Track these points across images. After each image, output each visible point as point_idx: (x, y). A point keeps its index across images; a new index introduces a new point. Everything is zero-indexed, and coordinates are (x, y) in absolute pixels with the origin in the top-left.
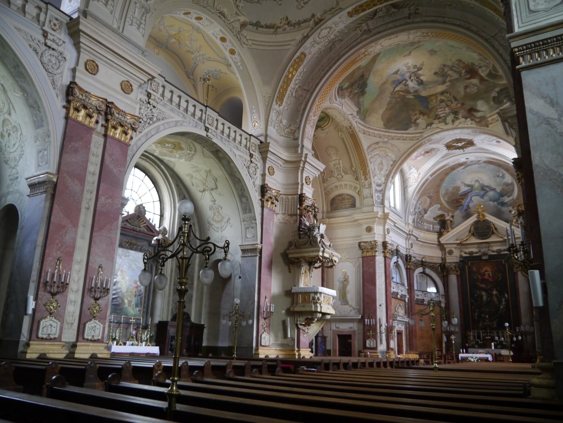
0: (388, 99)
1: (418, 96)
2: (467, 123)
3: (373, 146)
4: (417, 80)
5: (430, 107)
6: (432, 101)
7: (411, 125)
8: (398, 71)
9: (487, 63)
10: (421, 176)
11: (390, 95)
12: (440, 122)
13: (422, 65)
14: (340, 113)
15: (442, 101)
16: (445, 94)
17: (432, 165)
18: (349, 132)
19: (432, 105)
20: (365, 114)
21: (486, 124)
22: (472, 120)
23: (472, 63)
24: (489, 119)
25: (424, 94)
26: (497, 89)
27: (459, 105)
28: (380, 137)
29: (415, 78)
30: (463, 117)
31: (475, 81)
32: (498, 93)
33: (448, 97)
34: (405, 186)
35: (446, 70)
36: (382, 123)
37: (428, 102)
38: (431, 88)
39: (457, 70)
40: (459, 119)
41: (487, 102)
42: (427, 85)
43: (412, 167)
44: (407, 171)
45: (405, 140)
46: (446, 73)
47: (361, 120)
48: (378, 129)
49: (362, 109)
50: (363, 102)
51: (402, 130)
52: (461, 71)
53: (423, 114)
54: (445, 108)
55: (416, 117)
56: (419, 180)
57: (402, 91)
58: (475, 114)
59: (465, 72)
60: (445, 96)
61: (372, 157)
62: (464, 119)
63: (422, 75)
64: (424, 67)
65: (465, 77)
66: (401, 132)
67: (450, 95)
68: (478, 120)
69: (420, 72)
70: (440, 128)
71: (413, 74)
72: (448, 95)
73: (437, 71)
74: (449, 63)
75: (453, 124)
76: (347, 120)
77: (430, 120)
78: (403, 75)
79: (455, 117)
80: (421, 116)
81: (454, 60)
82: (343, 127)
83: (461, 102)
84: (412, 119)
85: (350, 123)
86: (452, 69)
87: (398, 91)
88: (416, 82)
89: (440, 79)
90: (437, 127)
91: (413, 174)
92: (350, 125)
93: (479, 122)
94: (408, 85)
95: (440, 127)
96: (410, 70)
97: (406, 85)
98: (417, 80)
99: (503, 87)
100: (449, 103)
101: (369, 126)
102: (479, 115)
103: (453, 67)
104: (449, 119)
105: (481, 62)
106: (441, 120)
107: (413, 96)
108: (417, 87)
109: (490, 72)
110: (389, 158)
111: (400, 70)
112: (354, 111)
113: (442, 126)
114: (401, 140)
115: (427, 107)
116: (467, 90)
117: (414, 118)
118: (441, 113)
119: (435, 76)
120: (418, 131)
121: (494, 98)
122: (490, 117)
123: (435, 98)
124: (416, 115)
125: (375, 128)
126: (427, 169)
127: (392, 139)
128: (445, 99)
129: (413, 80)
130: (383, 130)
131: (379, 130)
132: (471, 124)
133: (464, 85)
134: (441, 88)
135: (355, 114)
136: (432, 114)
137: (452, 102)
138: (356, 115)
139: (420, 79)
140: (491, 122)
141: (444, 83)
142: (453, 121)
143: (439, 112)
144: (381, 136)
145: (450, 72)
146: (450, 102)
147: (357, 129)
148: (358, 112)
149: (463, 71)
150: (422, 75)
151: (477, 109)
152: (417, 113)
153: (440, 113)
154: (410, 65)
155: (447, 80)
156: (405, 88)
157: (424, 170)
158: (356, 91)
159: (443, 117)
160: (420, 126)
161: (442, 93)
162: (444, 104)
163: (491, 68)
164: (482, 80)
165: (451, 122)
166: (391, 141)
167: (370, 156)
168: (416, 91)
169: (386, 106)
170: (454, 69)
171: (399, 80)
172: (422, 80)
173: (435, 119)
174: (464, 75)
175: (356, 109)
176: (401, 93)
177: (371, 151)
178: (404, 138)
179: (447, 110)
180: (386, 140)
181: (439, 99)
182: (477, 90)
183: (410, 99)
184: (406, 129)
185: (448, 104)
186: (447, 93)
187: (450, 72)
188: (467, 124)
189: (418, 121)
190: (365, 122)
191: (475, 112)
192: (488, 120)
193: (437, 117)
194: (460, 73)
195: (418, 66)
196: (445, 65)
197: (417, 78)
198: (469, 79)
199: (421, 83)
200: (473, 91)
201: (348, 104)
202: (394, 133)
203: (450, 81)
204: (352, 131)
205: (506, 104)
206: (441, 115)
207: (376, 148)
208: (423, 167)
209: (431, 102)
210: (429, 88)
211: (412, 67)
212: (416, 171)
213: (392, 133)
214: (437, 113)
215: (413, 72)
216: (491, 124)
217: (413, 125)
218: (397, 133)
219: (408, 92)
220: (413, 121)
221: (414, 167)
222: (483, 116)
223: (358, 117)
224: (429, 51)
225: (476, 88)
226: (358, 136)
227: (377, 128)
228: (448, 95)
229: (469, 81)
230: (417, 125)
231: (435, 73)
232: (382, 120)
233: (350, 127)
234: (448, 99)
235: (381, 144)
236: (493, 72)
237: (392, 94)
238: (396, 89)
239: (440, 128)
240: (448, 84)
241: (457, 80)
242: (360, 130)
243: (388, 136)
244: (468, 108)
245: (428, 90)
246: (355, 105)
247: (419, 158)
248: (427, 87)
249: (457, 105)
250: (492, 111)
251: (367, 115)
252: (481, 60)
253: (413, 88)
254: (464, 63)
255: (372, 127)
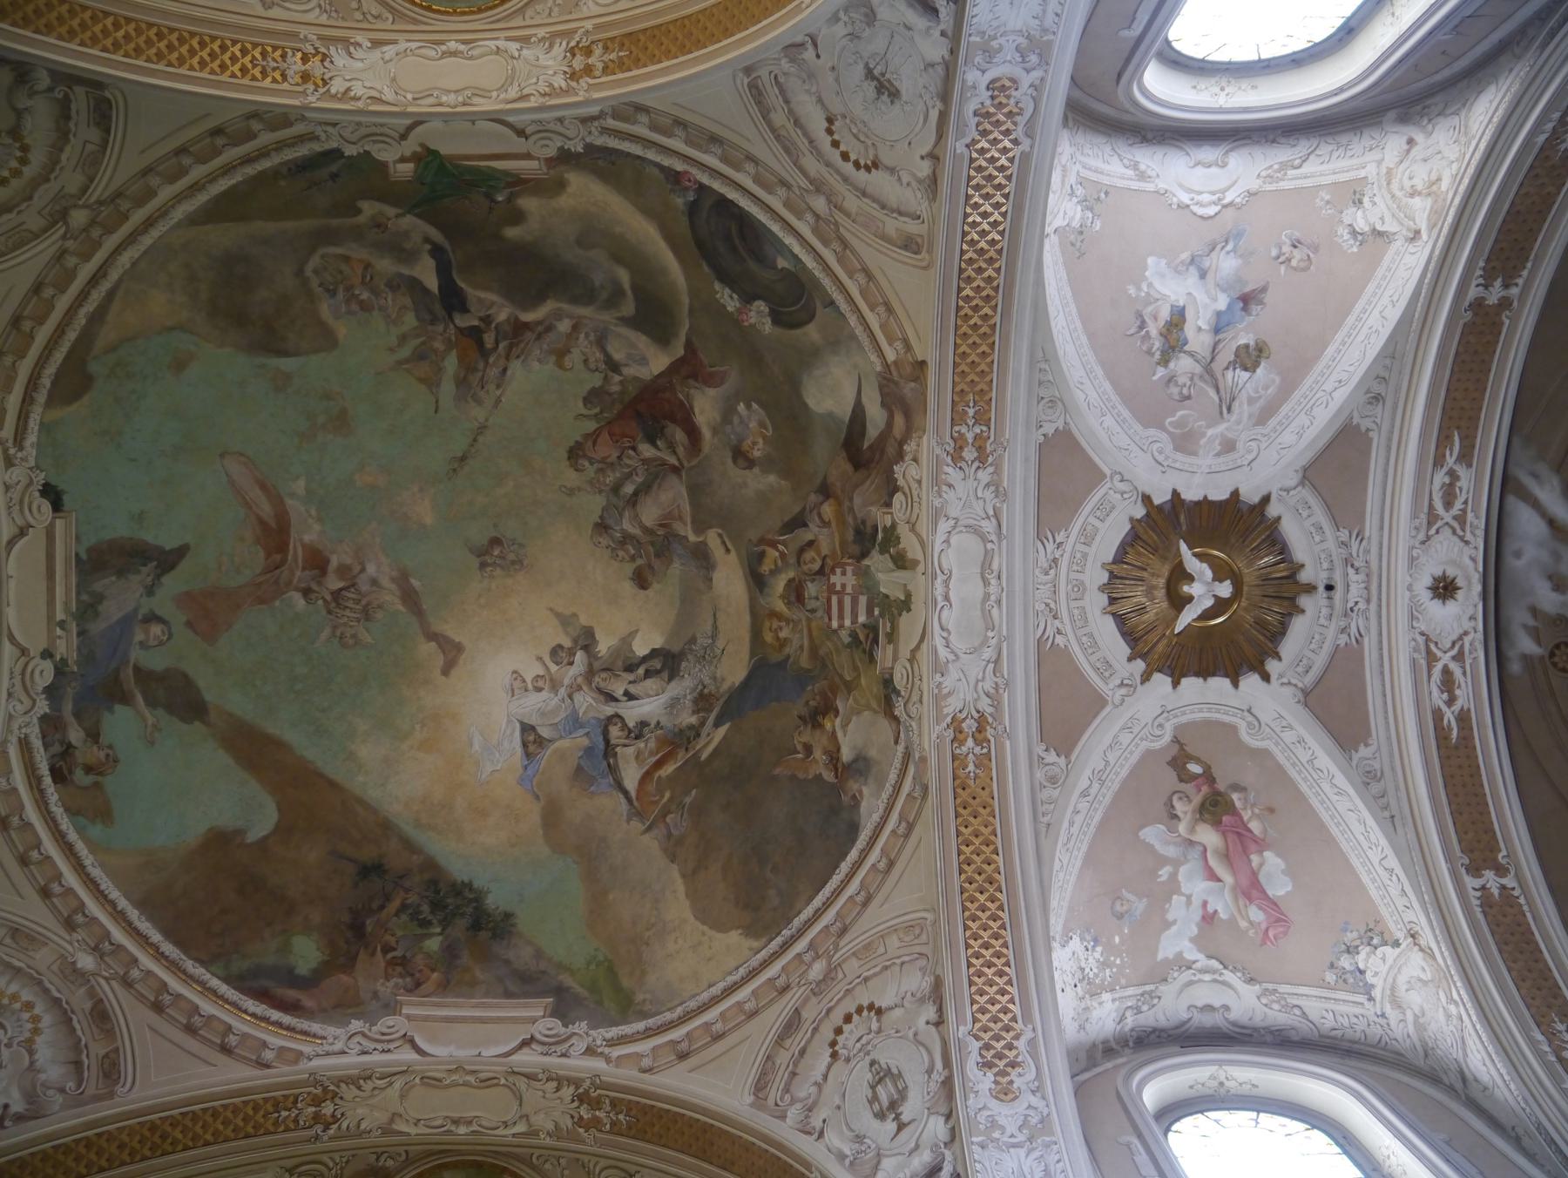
0: (651, 844)
1: (735, 705)
2: (914, 486)
3: (783, 1058)
4: (641, 671)
5: (805, 661)
6: (783, 643)
7: (845, 799)
8: (527, 729)
9: (575, 328)
10: (1428, 937)
11: (637, 826)
12: (892, 637)
13: (565, 621)
14: (430, 1082)
15: (796, 593)
16: (766, 568)
17: (1371, 822)
18: (615, 1128)
19: (801, 647)
20: (617, 988)
21: (916, 380)
22: (900, 456)
23: (587, 401)
24: (891, 356)
25: (734, 670)
26: (729, 300)
27: (828, 510)
28: (786, 988)
29: (631, 677)
30: (889, 505)
31: (705, 406)
32: (748, 298)
33: (782, 555)
34: (1459, 1086)
35: (627, 526)
36: (734, 937)
37: (782, 665)
38: (715, 627)
39: (639, 480)
40: (894, 526)
41: (810, 357)
42: (693, 640)
43: (1345, 962)
44: (1370, 1010)
45: (891, 864)
46: (646, 530)
47: (617, 1025)
48: (742, 971)
49: (567, 980)
50: (539, 954)
51: (844, 855)
52: (645, 461)
53: (816, 716)
54: (831, 589)
55: (818, 754)
56: (1443, 955)
57: (659, 764)
58: (872, 433)
59: (652, 441)
60: (775, 572)
61: (810, 1110)
62: (898, 499)
63: (627, 641)
64: (584, 620)
65: (680, 450)
66: (845, 867)
67: (773, 545)
68: (899, 421)
69: (604, 646)
70: (918, 647)
71: (597, 679)
72: (772, 553)
73: (629, 568)
74: (594, 504)
75: (915, 563)
76: (522, 1083)
77: (868, 683)
78: (575, 722)
79: (884, 550)
80: (828, 726)
81: (571, 477)
82: (572, 1136)
83: (813, 498)
84: (819, 777)
85: (560, 1081)
86: (633, 500)
87: (646, 777)
88: (651, 684)
89: (676, 568)
90: (912, 659)
91: (1402, 986)
92: (567, 1092)
93: (908, 415)
94: (643, 724)
95: (913, 646)
96: (566, 681)
97: (638, 731)
98: (641, 671)
99: (706, 269)
100: (812, 561)
101: (679, 1011)
102: (875, 414)
103: (616, 489)
104: (889, 581)
105: (574, 358)
106: (884, 627)
107: (717, 725)
108: (682, 687)
109: (635, 323)
110: (898, 1012)
111: (533, 721)
112: (534, 1020)
113: (908, 627)
114: (879, 888)
115: (803, 679)
116: (757, 454)
117: (819, 766)
118: (850, 617)
119: (656, 586)
120: (893, 777)
121: (778, 319)
122: (881, 355)
123: (775, 624)
124: (808, 749)
125: (715, 990)
126: (1399, 870)
127: (844, 931)
128: (791, 574)
129: (633, 689)
130: (763, 954)
131: (753, 974)
132: (915, 460)
133: (729, 461)
134: (729, 581)
135: (549, 1026)
136: (843, 664)
137: (811, 544)
138: (563, 1030)
139: (645, 659)
140: (899, 345)
141: (702, 557)
142: (901, 562)
143: (841, 626)
144: (780, 982)
145: (650, 513)
146: (809, 555)
147: (627, 1076)
148: (564, 1010)
149: (647, 450)
150: (627, 641)
151: (847, 419)
152: (806, 736)
153: (847, 623)
154: (532, 670)
155: (692, 538)
156: (652, 744)
157: (1394, 891)
158: (433, 944)
159: (870, 612)
160: (873, 753)
161: (757, 581)
162: (811, 589)
163: (606, 317)
164: (689, 369)
165: (901, 576)
166: (849, 944)
167: (794, 1113)
168: (702, 701)
169: (675, 872)
170: (629, 489)
171: (589, 751)
172: (654, 653)
173: (872, 660)
174: (672, 447)
175: (536, 1008)
176: (669, 769)
177: (787, 1090)
178: (882, 865)
179: (845, 579)
180: (817, 970)
181: (780, 606)
182: (755, 406)
183: (724, 738)
184: (853, 829)
185: (816, 566)
186: (762, 555)
187: (650, 513)
188: (919, 482)
189: (846, 755)
190: (644, 1015)
191: (863, 434)
192: (895, 362)
193: (866, 642)
194: (657, 473)
195: (567, 643)
196: (602, 527)
197: (630, 668)
198: (693, 433)
199: (666, 663)
200: (762, 425)
201: (426, 1019)
202: (827, 904)
203: (700, 528)
204: (614, 1103)
205: (796, 257)
206: (862, 619)
207: (803, 1052)
208: (1373, 893)
209: (787, 650)
210: (714, 637)
211: (554, 668)
212: (1388, 949)
213: (818, 914)
214: (845, 637)
215: (590, 673)
216: (908, 347)
217: (853, 786)
218: (837, 893)
219: (679, 740)
220: (829, 776)
221: (1351, 950)
222: (881, 388)
223: (581, 1027)
224: (483, 565)
225: (741, 407)
226: (659, 1098)
227: (731, 979)
228: (772, 553)
229: (706, 433)
230: (861, 766)
231: (641, 580)
232: (721, 927)
233: (582, 1098)
234: (792, 560)
235: (808, 1014)
236: (629, 308)
237: (637, 813)
238: (631, 783)
239: (918, 647)
240: (712, 538)
241: (695, 491)
242: (646, 1062)
243: (811, 946)
244: (849, 467)
245: (720, 644)
246: (509, 995)
247: (1279, 886)
248: (703, 641)
249: (825, 524)
250: (853, 337)
251: (626, 982)
252: (561, 354)
253: (673, 704)
254: (594, 437)
255: (705, 996)
